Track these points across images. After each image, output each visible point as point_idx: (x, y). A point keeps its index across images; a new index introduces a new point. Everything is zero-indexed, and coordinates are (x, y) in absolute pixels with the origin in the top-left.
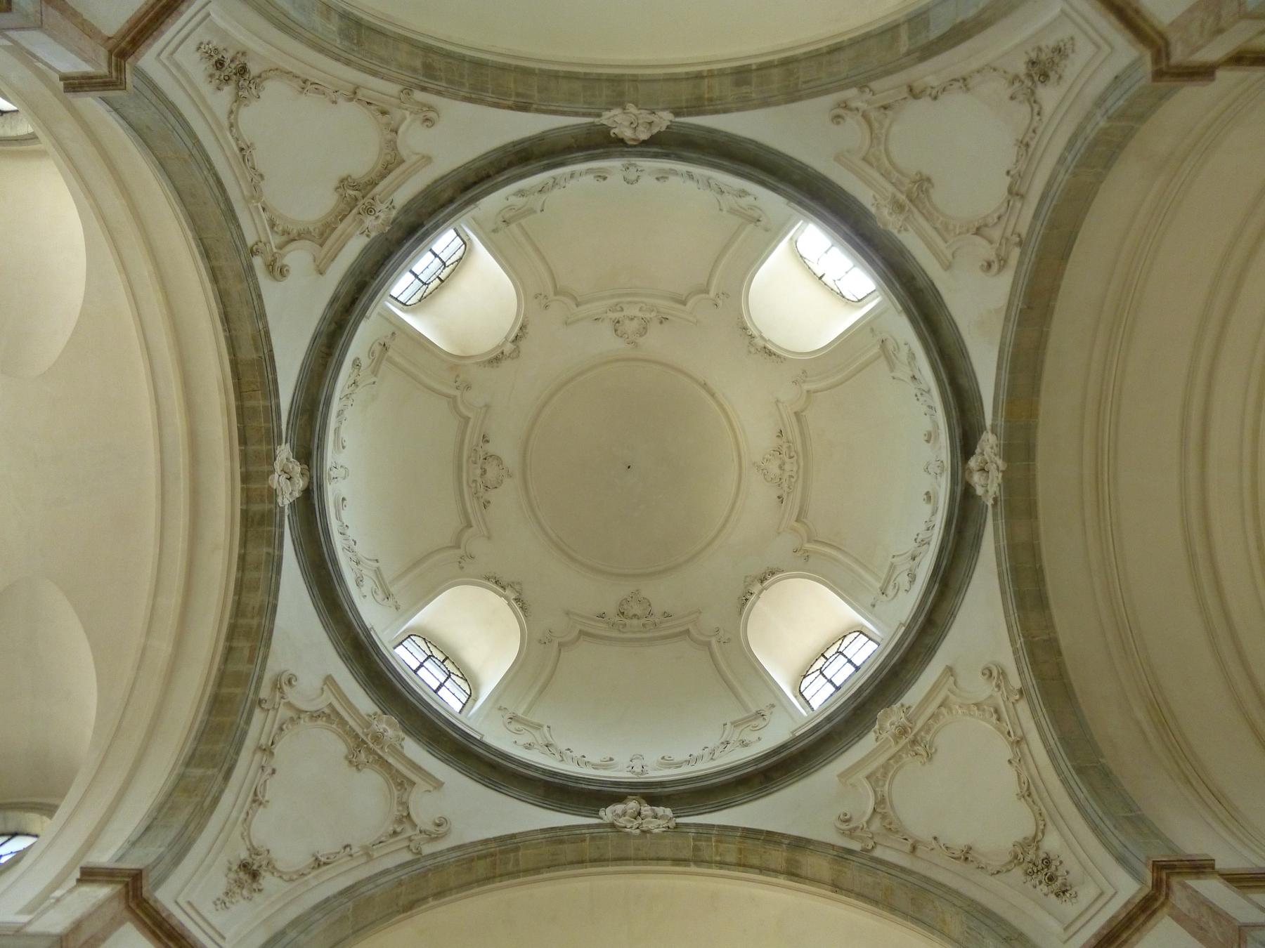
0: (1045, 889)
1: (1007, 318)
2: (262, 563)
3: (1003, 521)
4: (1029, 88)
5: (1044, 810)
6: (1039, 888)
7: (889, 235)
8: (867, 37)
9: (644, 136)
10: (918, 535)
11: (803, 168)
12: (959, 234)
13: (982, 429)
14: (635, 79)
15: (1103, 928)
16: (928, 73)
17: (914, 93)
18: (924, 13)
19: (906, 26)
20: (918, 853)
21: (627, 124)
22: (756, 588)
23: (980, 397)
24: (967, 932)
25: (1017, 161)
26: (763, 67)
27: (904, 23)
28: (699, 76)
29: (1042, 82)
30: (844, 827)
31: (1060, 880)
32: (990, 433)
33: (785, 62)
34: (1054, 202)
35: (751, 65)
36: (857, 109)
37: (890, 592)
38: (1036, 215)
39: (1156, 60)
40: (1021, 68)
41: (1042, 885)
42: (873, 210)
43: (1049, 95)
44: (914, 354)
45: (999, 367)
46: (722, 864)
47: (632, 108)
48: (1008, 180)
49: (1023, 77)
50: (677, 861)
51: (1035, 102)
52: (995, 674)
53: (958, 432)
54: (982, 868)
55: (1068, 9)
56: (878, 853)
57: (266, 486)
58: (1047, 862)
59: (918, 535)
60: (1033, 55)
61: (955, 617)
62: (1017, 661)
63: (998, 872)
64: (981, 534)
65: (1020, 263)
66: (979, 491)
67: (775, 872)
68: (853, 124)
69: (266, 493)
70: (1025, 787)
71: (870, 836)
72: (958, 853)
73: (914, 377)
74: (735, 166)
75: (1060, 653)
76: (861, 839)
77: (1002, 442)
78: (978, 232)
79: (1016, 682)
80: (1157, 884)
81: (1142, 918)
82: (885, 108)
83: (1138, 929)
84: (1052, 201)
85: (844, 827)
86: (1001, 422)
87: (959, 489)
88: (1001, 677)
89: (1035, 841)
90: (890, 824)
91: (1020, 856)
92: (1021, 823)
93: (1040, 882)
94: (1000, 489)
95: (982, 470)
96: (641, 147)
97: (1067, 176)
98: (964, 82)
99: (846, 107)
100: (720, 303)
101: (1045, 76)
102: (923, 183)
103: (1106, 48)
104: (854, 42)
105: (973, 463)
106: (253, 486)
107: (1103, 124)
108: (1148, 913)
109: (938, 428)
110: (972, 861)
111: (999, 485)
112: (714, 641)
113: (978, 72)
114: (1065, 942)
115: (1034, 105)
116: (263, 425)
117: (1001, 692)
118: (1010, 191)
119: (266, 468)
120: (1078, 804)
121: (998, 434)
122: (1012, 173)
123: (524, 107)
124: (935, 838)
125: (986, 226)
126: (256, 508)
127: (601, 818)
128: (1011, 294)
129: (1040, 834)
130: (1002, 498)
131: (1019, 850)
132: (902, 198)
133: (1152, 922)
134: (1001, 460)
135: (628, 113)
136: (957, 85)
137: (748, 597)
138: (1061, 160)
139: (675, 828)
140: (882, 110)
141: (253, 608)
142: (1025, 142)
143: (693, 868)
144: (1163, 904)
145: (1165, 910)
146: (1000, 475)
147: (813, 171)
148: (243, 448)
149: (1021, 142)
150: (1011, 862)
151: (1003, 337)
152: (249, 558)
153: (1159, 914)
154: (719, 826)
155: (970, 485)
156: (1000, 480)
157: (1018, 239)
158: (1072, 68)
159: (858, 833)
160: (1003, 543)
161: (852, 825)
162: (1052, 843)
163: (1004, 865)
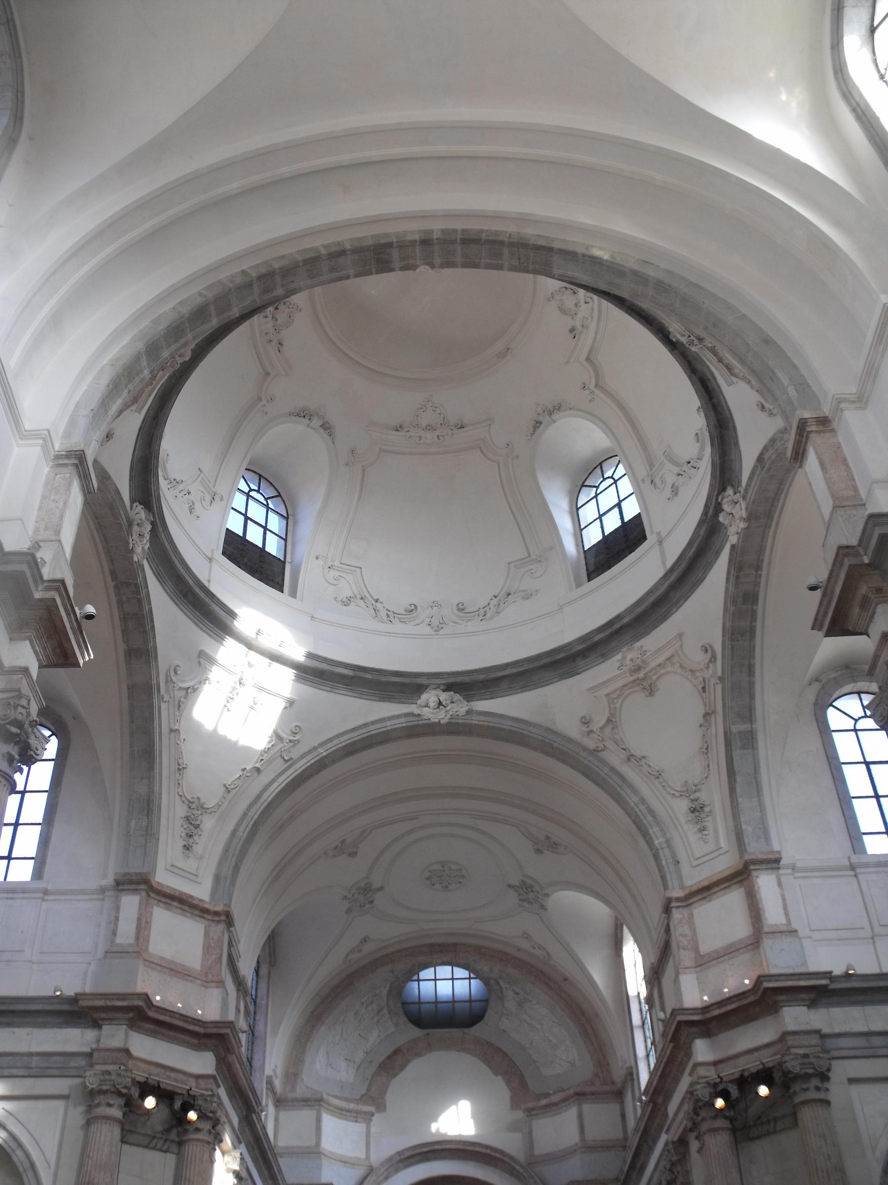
0: (184, 835)
1: (548, 730)
2: (338, 272)
3: (404, 725)
4: (690, 796)
5: (223, 807)
6: (183, 830)
7: (617, 650)
8: (752, 696)
9: (721, 518)
10: (381, 603)
11: (677, 605)
12: (610, 707)
13: (468, 698)
14: (767, 527)
15: (186, 894)
16: (718, 727)
17: (706, 715)
18: (753, 746)
19: (750, 729)
20: (173, 734)
21: (734, 512)
22: (316, 422)
23: (493, 698)
24: (144, 800)
25: (649, 766)
26: (754, 614)
27: (752, 727)
28: (759, 568)
29: (690, 809)
30: (172, 673)
31: (191, 841)
32: (466, 709)
33: (752, 631)
34: (618, 789)
35: (757, 605)
36: (708, 668)
37: (333, 573)
38: (612, 769)
39: (678, 899)
40: (703, 796)
41: (184, 831)
42: (638, 644)
43: (681, 806)
44: (528, 598)
45: (514, 719)
46: (120, 603)
47: (742, 525)
48: (638, 754)
49: (697, 795)
50: (113, 573)
51: (681, 795)
52: (298, 737)
53: (467, 679)
54: (179, 784)
55: (722, 851)
56: (163, 706)
57: (418, 262)
58: (197, 827)
59: (381, 603)
60: (707, 809)
61: (331, 691)
62: (310, 752)
63: (181, 796)
64: (393, 700)
65: (585, 749)
66: (424, 697)
67: (126, 641)
68: (700, 658)
69: (411, 261)
70: (233, 787)
71: (172, 696)
72: (180, 761)
73: (509, 594)
74: (687, 559)
75: (317, 774)
76: (167, 690)
77: (461, 721)
78: (609, 721)
79: (295, 753)
80: (217, 913)
81: (197, 912)
82: (704, 688)
83: (192, 913)
84: (619, 786)
85: (172, 673)
86: (475, 720)
87: (424, 681)
88: (296, 742)
89: (202, 808)
90: (183, 703)
91: (194, 806)
92: (211, 797)
93: (185, 829)
94: (425, 719)
95: (440, 703)
96: (715, 504)
97: (632, 804)
98: (706, 750)
99: (710, 661)
100: (587, 392)
101: (693, 810)
102: (651, 691)
103: (695, 863)
104: (752, 685)
105: (444, 696)
106: (418, 249)
107: (656, 842)
108: (201, 914)
109: (468, 620)
110: (180, 774)
111: (429, 719)
112: (264, 402)
113: (708, 765)
114: (166, 869)
115: (680, 793)
116: (483, 261)
117: (286, 745)
118: (632, 755)
119: (437, 261)
120: (235, 831)
121: (467, 717)
122: (643, 760)
123: (760, 459)
124: (184, 740)
125: (613, 728)
126: (395, 254)
127: (131, 509)
128: (564, 736)
129: (209, 811)
130: (421, 722)
131: (196, 804)
132: (641, 675)
133: (198, 918)
134: (448, 721)
135: (741, 520)
136: (705, 745)
137: (308, 417)
138: (643, 801)
139: (139, 565)
140: (703, 685)
141: (292, 282)
142: (660, 776)
143: (111, 584)
144: (208, 920)
145: (206, 922)
146: (436, 721)
147: (673, 612)
148: (459, 242)
149: (660, 774)
150: (189, 801)
151: (535, 725)
152: (341, 259)
153: (203, 920)
154: (148, 591)
155: (427, 688)
156: (433, 720)
157: (600, 749)
158: (691, 830)
159: (171, 685)
160: (389, 725)
161: (174, 679)
162: (208, 823)
163: (185, 797)
